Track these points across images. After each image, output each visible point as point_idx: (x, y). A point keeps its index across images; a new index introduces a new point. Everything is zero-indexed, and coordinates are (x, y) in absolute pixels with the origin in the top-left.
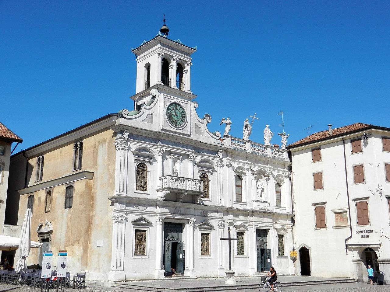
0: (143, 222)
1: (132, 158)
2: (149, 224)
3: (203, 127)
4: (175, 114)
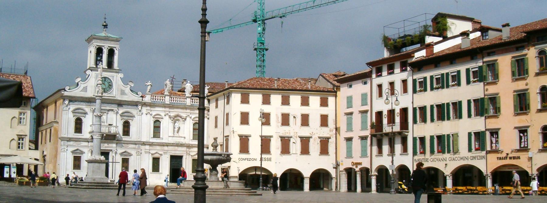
0: (78, 151)
1: (71, 115)
2: (82, 153)
3: (127, 90)
4: (107, 84)
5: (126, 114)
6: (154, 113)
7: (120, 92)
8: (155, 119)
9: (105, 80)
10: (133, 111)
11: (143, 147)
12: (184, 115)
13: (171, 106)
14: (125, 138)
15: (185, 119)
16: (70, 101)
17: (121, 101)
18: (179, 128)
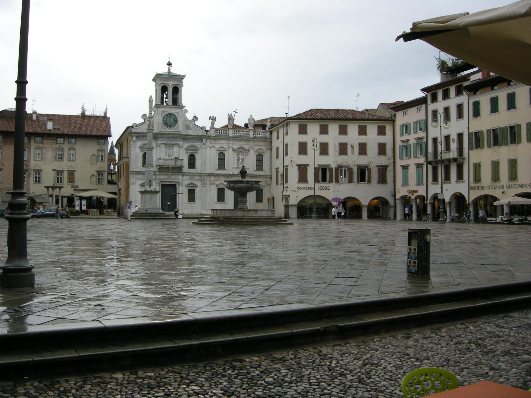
5: (191, 148)
6: (218, 146)
7: (185, 127)
8: (219, 152)
9: (170, 117)
10: (198, 144)
11: (207, 179)
12: (246, 147)
13: (234, 138)
14: (192, 171)
15: (249, 151)
16: (138, 137)
17: (186, 135)
18: (243, 160)
